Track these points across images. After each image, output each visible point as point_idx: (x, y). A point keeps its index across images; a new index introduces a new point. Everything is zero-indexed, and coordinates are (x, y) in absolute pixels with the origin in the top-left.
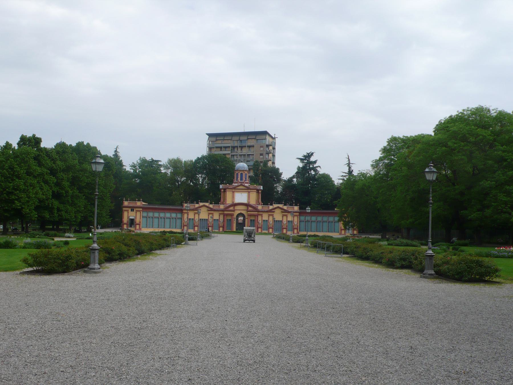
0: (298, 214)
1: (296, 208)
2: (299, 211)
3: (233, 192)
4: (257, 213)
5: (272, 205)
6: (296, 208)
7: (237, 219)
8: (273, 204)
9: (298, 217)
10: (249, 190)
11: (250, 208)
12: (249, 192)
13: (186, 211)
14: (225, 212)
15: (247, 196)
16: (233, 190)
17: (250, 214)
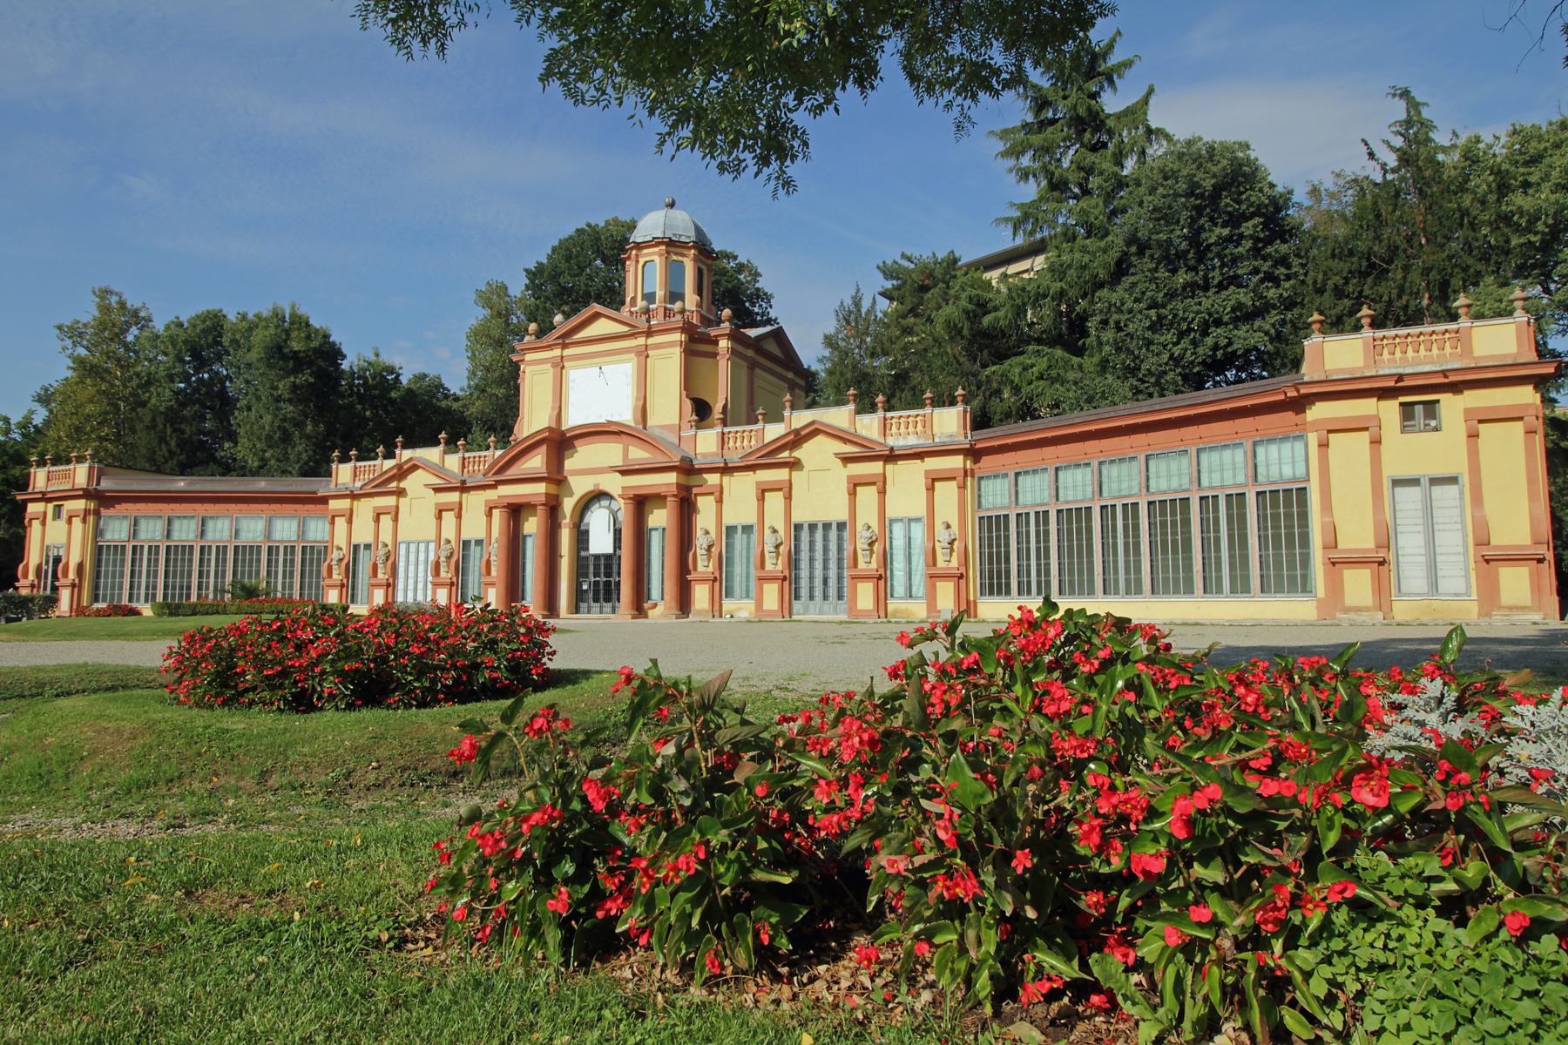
0: (957, 462)
1: (949, 422)
2: (963, 440)
3: (560, 365)
4: (671, 478)
5: (779, 418)
6: (949, 422)
7: (581, 538)
8: (786, 413)
9: (962, 487)
10: (641, 341)
11: (638, 454)
12: (643, 354)
13: (344, 504)
14: (504, 490)
15: (630, 380)
16: (557, 352)
17: (631, 493)
